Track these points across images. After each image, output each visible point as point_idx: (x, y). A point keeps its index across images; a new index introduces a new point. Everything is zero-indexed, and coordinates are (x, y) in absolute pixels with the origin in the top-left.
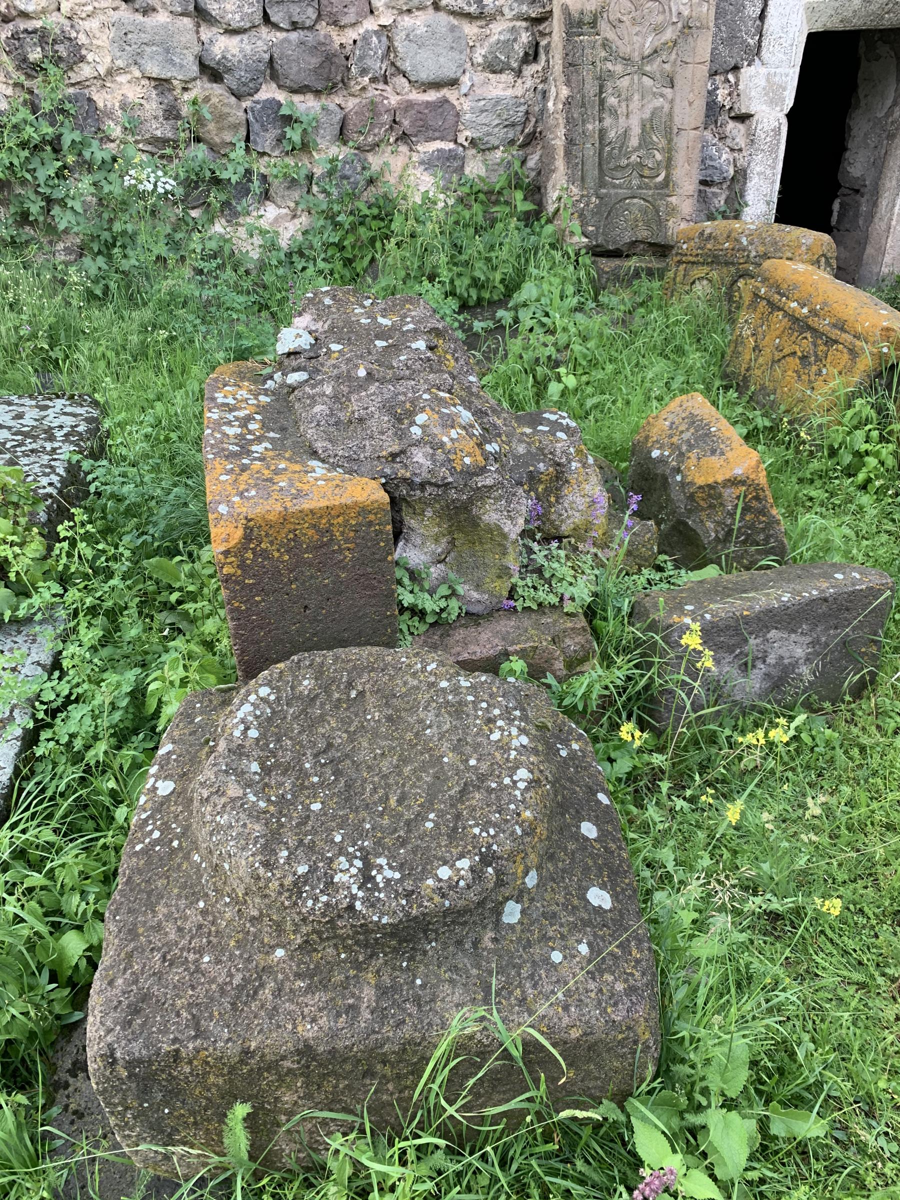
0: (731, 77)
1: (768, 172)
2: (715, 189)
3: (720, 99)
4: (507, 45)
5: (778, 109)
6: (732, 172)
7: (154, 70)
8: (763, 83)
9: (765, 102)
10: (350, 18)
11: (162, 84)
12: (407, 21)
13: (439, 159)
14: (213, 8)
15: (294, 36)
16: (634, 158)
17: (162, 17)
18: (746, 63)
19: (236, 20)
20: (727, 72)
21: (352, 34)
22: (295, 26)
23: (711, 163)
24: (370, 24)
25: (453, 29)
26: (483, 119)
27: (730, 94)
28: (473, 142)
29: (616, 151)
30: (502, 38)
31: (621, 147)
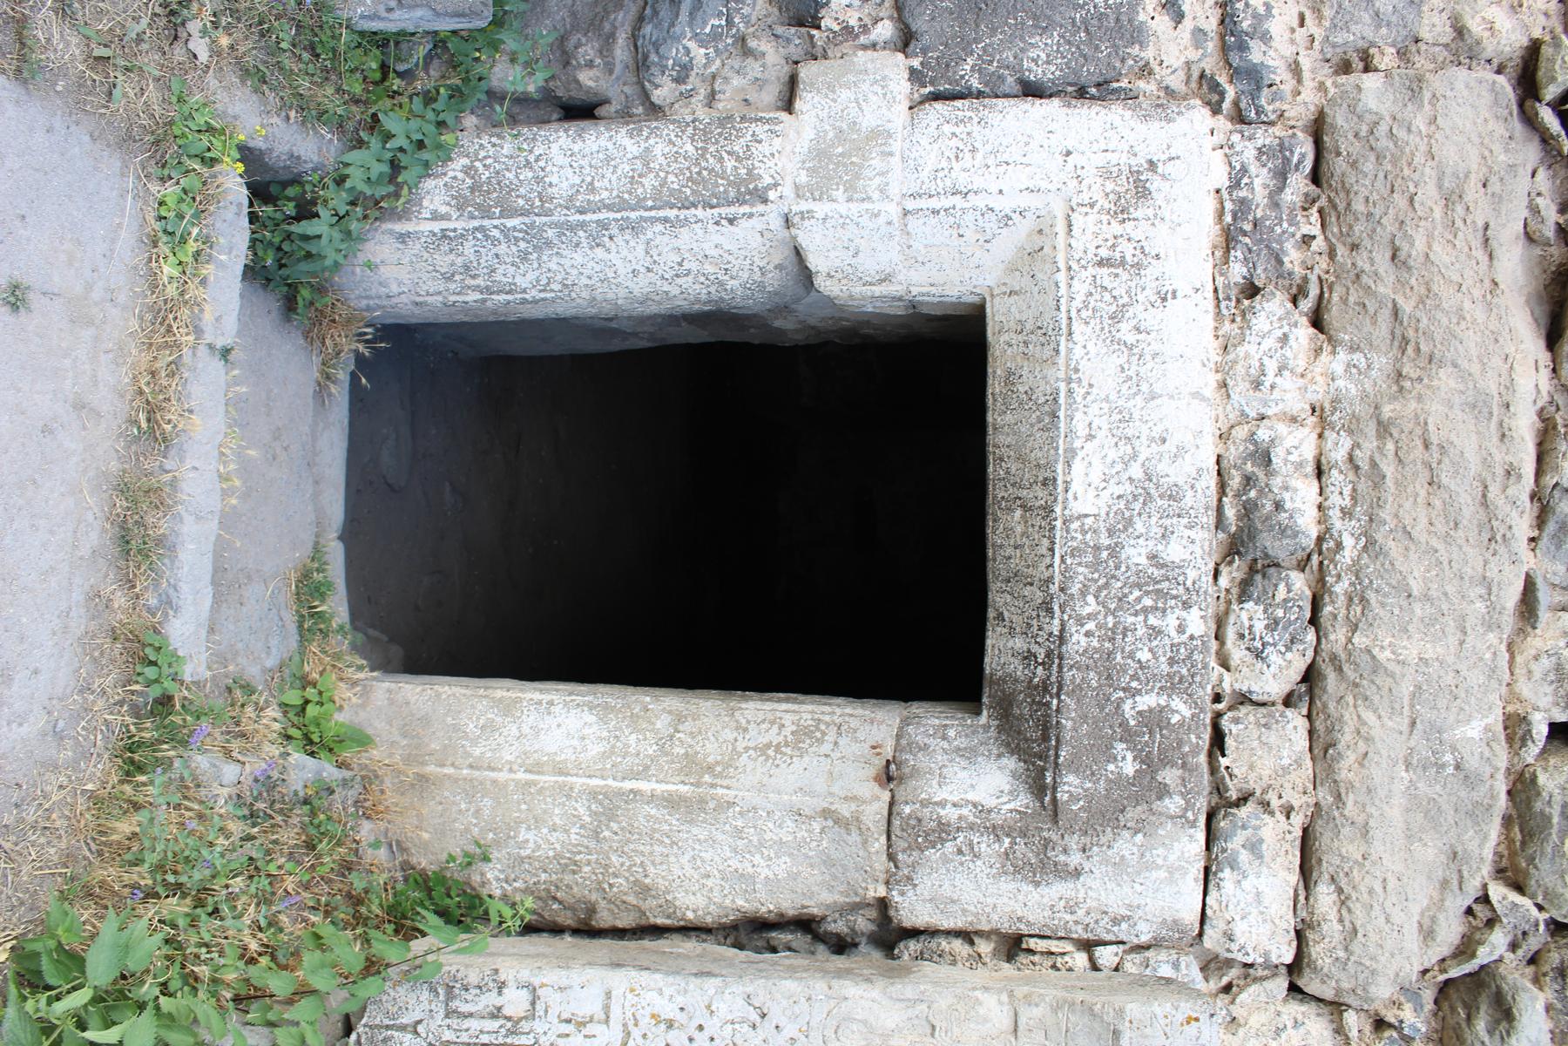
0: (885, 30)
1: (649, 182)
5: (803, 178)
8: (868, 121)
9: (820, 137)
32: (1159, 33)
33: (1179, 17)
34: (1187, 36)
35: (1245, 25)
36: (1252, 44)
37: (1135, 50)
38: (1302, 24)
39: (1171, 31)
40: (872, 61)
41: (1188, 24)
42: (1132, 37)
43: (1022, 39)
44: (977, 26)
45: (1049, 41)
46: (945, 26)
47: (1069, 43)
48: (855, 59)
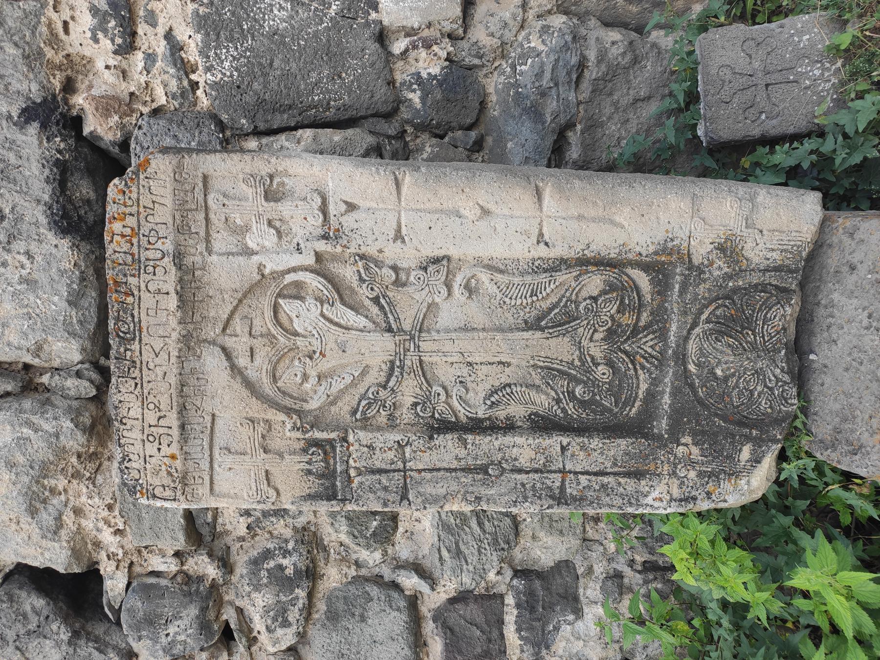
0: (399, 46)
2: (592, 55)
3: (435, 70)
6: (558, 21)
13: (531, 629)
16: (597, 351)
18: (373, 15)
20: (390, 54)
23: (548, 75)
26: (470, 550)
27: (428, 46)
29: (579, 390)
30: (344, 528)
31: (572, 378)
32: (184, 24)
33: (169, 36)
34: (161, 21)
35: (112, 23)
36: (106, 7)
37: (202, 10)
38: (66, 24)
39: (174, 26)
40: (406, 18)
41: (161, 30)
42: (206, 21)
43: (293, 27)
44: (328, 41)
45: (271, 23)
46: (353, 43)
47: (256, 20)
48: (419, 19)
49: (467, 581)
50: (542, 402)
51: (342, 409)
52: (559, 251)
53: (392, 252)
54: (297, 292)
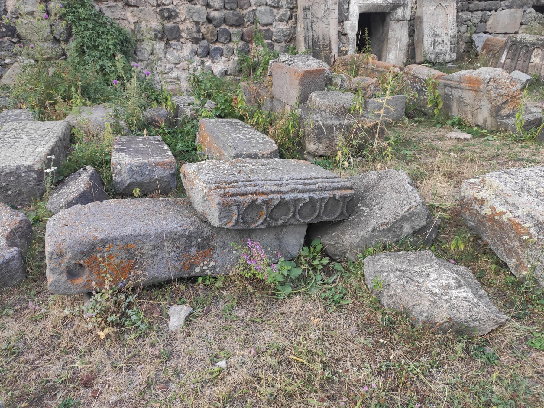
4: (285, 15)
7: (196, 19)
8: (350, 25)
10: (246, 7)
11: (197, 23)
12: (259, 8)
14: (212, 4)
15: (231, 12)
17: (198, 6)
19: (217, 7)
21: (245, 12)
22: (231, 9)
24: (250, 9)
25: (271, 10)
26: (279, 34)
28: (276, 41)
49: (275, 33)
50: (315, 37)
51: (313, 11)
52: (331, 37)
53: (330, 18)
54: (325, 6)
